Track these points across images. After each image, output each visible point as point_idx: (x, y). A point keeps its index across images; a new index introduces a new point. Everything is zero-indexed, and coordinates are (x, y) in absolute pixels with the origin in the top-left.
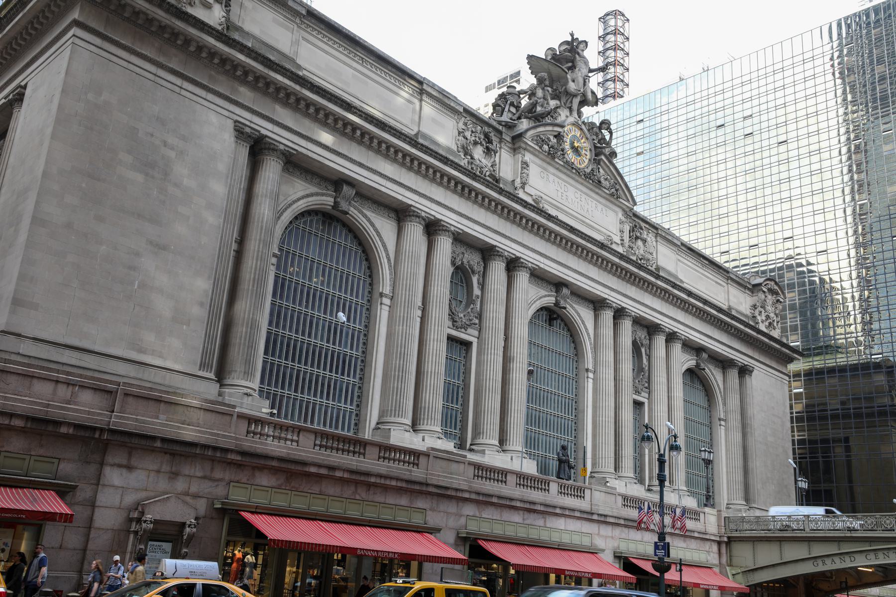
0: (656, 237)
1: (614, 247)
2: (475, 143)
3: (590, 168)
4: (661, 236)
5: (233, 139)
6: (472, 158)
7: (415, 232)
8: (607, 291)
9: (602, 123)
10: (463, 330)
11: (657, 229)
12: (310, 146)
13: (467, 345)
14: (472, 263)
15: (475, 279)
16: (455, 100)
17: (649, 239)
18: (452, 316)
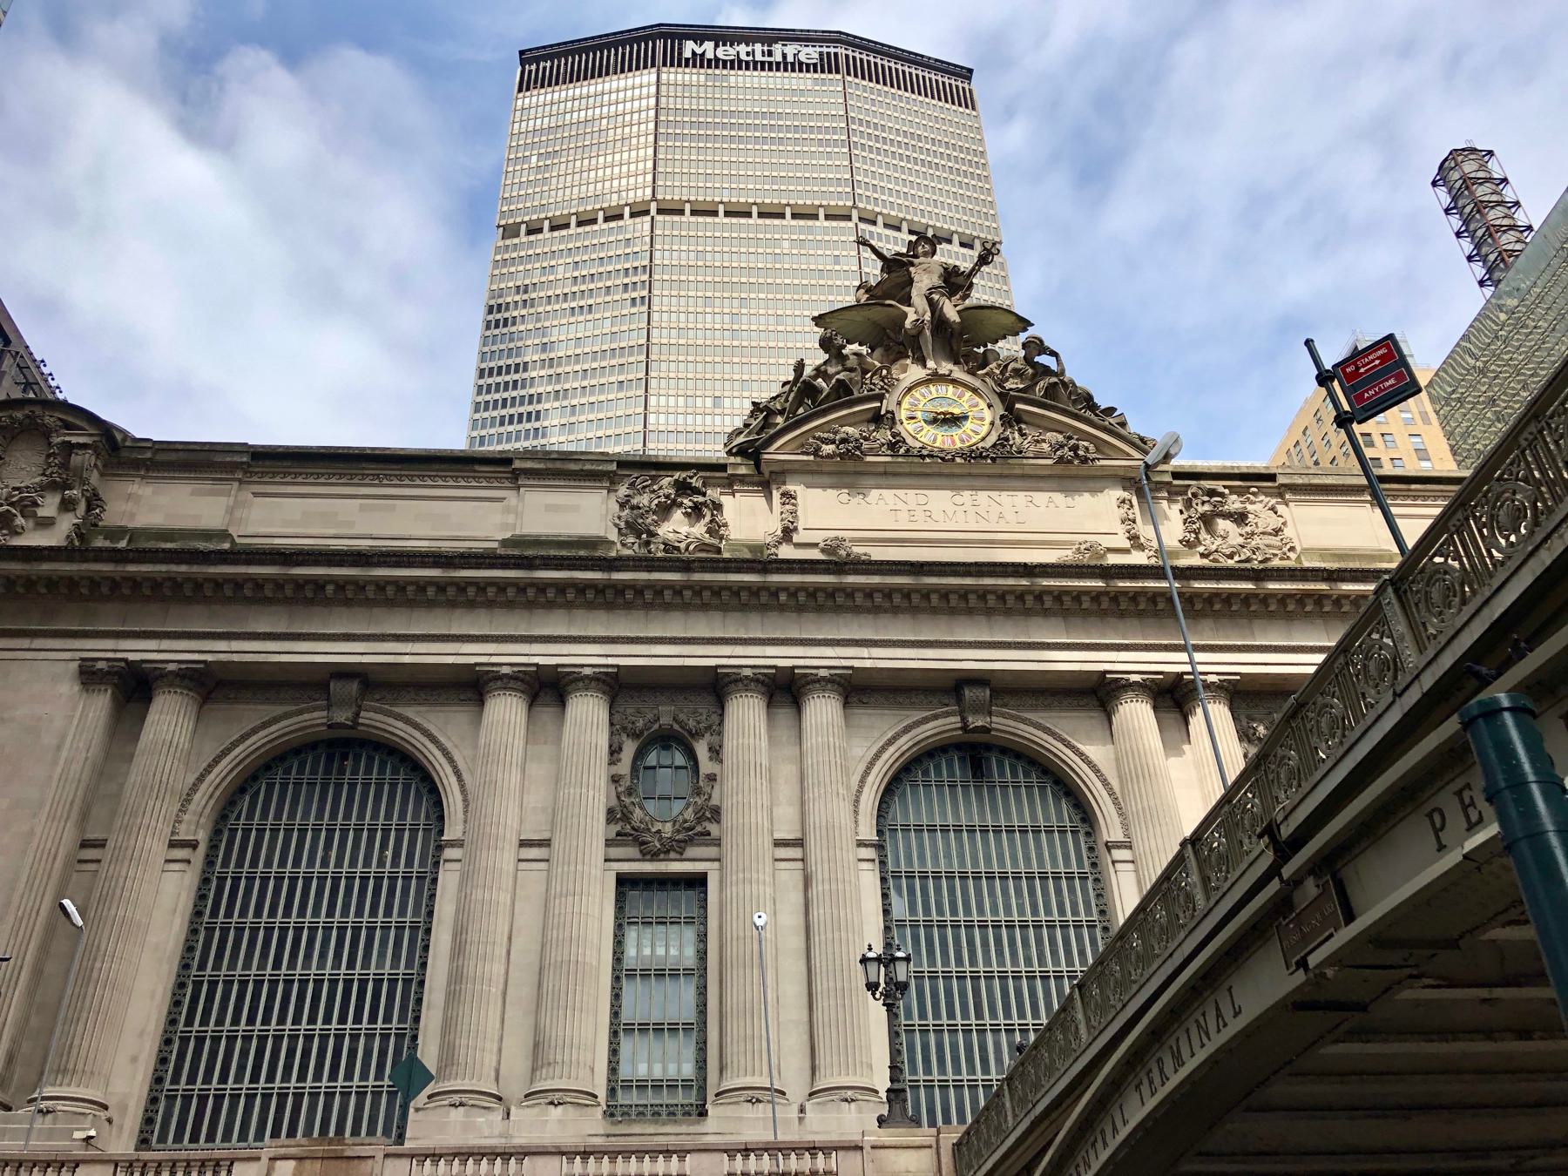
0: (1281, 495)
1: (1113, 559)
2: (665, 510)
3: (993, 439)
4: (1294, 488)
5: (77, 688)
6: (652, 534)
7: (506, 710)
9: (1024, 346)
10: (672, 855)
11: (1271, 477)
12: (236, 645)
13: (697, 882)
14: (682, 717)
15: (701, 749)
16: (605, 458)
17: (1250, 507)
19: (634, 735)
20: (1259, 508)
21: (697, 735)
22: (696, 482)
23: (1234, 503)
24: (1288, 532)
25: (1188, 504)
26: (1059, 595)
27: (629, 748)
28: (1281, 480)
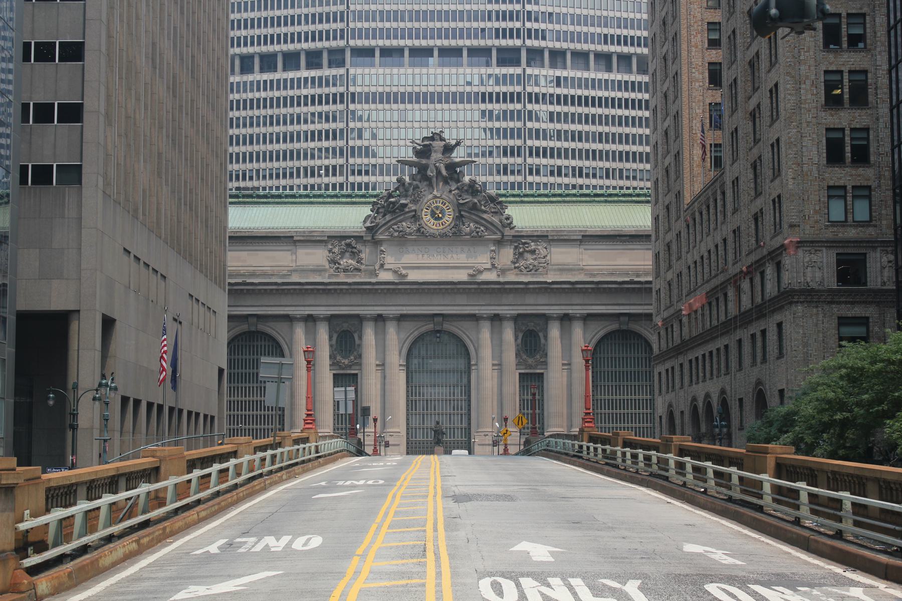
2: (342, 254)
4: (553, 240)
6: (339, 264)
8: (477, 308)
11: (547, 236)
13: (356, 374)
15: (356, 336)
18: (334, 364)
19: (336, 332)
20: (541, 248)
21: (355, 332)
22: (353, 243)
23: (533, 246)
24: (548, 258)
25: (516, 248)
26: (464, 289)
27: (335, 337)
28: (550, 238)
